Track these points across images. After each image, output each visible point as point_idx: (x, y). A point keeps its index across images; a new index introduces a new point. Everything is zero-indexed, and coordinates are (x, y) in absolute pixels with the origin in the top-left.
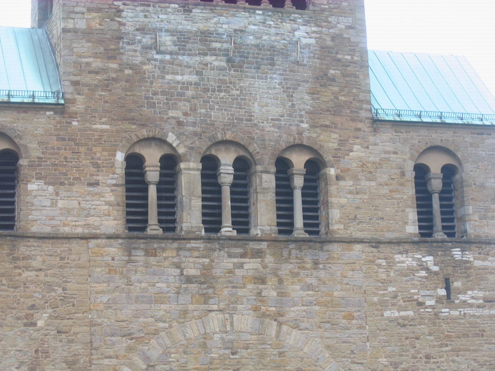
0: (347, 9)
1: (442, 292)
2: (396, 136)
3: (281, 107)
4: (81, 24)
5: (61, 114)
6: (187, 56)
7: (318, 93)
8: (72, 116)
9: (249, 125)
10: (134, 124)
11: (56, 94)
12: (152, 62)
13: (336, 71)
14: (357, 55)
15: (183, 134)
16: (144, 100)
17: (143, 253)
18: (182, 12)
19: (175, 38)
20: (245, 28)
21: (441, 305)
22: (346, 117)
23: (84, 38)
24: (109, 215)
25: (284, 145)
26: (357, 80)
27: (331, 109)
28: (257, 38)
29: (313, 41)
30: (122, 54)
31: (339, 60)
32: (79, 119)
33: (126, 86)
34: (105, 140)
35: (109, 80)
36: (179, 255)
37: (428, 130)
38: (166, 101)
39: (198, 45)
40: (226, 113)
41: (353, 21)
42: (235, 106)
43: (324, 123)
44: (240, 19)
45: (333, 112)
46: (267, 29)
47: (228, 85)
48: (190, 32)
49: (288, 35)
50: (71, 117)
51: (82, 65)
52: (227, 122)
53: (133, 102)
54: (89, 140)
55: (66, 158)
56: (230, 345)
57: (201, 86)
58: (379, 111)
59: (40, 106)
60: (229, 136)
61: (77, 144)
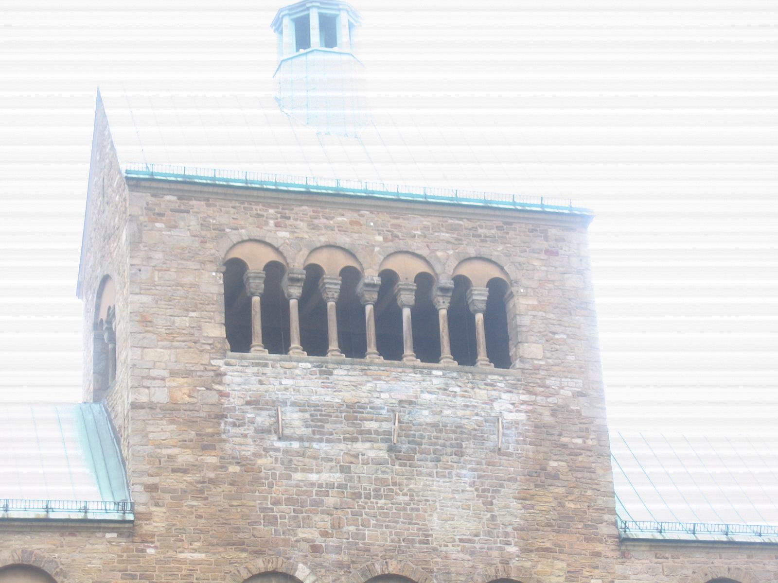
0: (575, 365)
2: (657, 563)
3: (475, 521)
4: (161, 396)
5: (129, 537)
6: (326, 442)
7: (532, 497)
8: (147, 539)
9: (425, 550)
10: (244, 550)
11: (121, 506)
12: (271, 453)
13: (560, 463)
14: (591, 437)
15: (320, 565)
16: (259, 513)
18: (318, 375)
19: (307, 415)
20: (416, 397)
22: (578, 535)
23: (164, 417)
26: (593, 476)
27: (554, 523)
28: (435, 413)
29: (522, 417)
30: (224, 441)
31: (564, 446)
32: (157, 544)
33: (231, 492)
34: (198, 576)
35: (204, 482)
37: (708, 553)
38: (293, 514)
39: (343, 425)
40: (387, 531)
41: (584, 385)
42: (402, 520)
43: (542, 544)
44: (408, 385)
45: (556, 528)
46: (450, 398)
47: (391, 487)
49: (483, 408)
50: (143, 542)
51: (162, 460)
52: (390, 546)
53: (242, 517)
54: (173, 577)
57: (349, 490)
58: (629, 525)
59: (96, 525)
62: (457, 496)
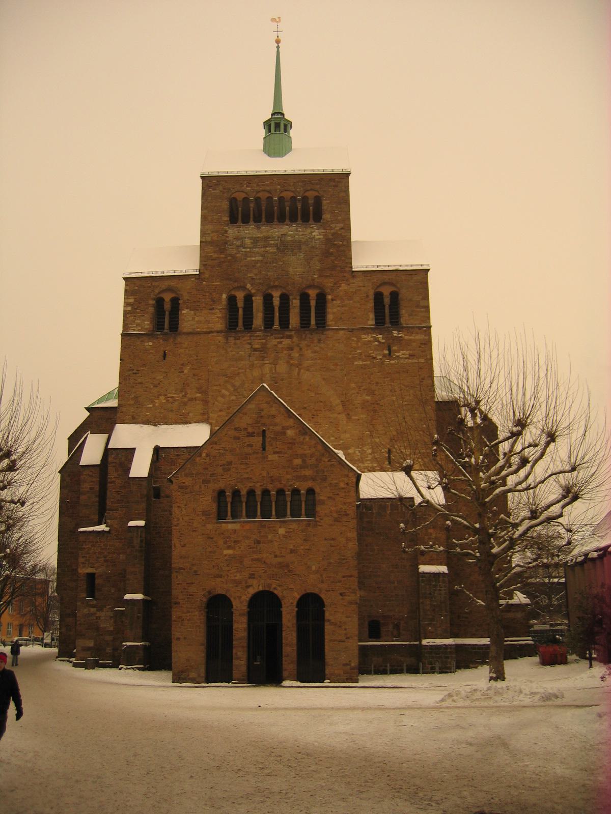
1: (386, 352)
4: (209, 239)
17: (233, 338)
21: (384, 358)
24: (218, 322)
25: (304, 286)
30: (226, 250)
36: (251, 339)
48: (259, 237)
50: (202, 280)
55: (199, 298)
56: (274, 379)
60: (276, 283)
61: (205, 292)
62: (298, 261)
